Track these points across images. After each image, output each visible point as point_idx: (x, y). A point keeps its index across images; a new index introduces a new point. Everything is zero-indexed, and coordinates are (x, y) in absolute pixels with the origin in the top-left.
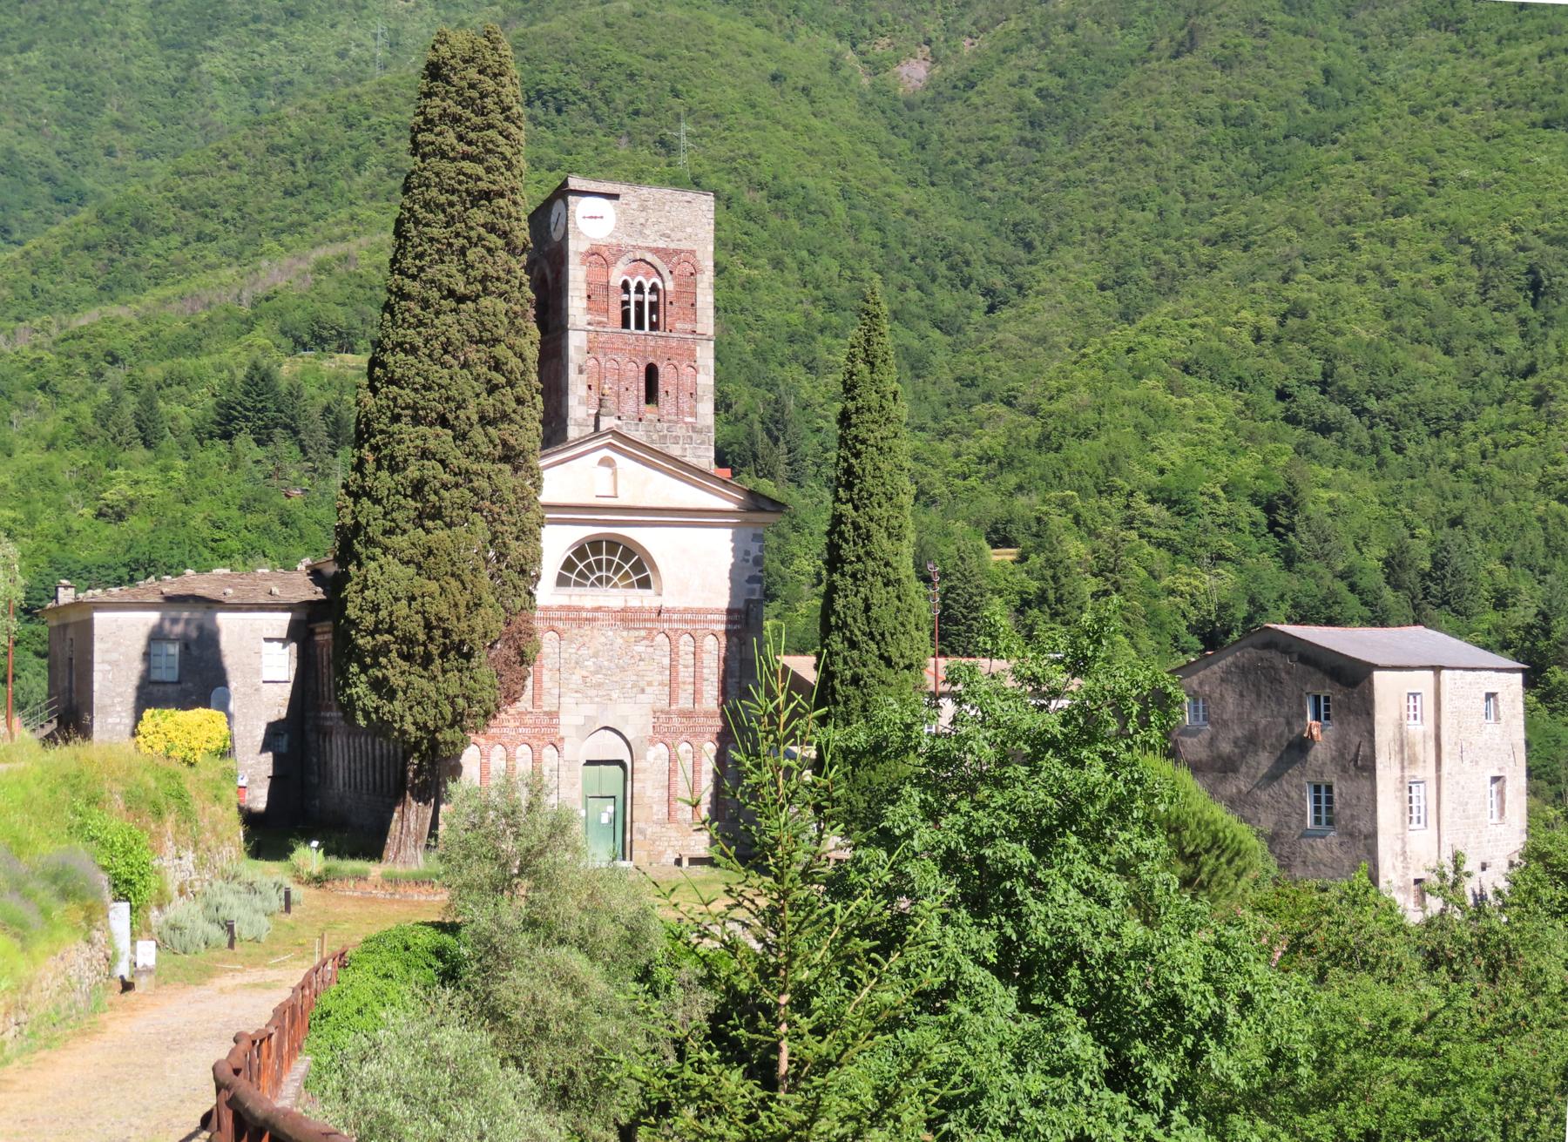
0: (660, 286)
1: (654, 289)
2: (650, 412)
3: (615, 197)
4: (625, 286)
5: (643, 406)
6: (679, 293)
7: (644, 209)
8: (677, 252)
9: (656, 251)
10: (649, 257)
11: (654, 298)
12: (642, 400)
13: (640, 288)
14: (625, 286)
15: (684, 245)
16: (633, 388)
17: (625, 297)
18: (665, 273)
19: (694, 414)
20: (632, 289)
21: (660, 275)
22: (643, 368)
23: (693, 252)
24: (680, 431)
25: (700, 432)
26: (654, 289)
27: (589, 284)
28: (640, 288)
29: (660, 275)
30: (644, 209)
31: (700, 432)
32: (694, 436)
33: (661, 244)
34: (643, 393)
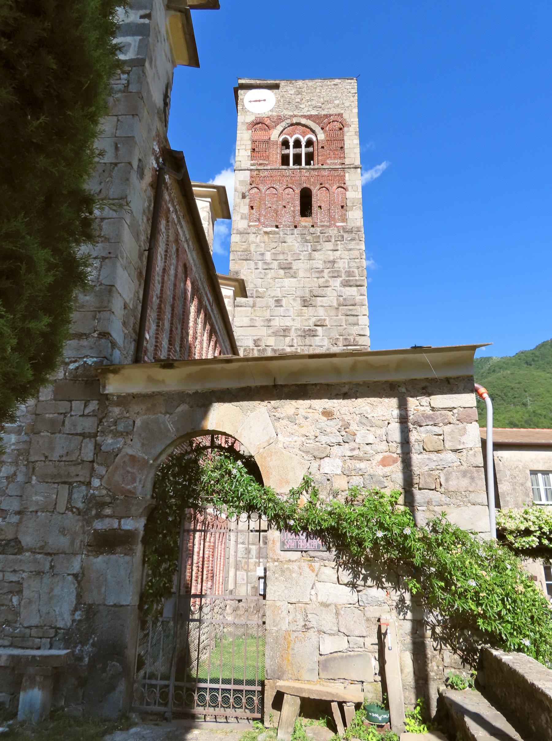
0: (314, 139)
1: (309, 143)
2: (306, 222)
3: (276, 87)
4: (285, 144)
5: (298, 218)
6: (329, 141)
7: (299, 93)
8: (326, 116)
9: (309, 117)
10: (303, 121)
11: (311, 149)
12: (298, 213)
13: (297, 144)
14: (285, 144)
15: (333, 111)
16: (290, 207)
17: (286, 152)
18: (317, 129)
19: (344, 220)
20: (291, 144)
21: (313, 132)
22: (298, 191)
23: (340, 115)
24: (332, 232)
25: (350, 231)
26: (309, 143)
27: (254, 142)
28: (297, 144)
29: (313, 132)
30: (299, 93)
31: (350, 231)
32: (346, 235)
33: (314, 113)
34: (298, 208)
